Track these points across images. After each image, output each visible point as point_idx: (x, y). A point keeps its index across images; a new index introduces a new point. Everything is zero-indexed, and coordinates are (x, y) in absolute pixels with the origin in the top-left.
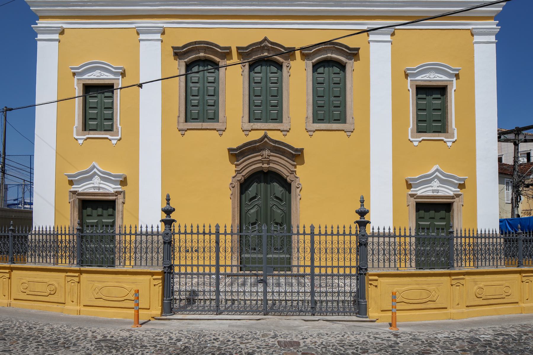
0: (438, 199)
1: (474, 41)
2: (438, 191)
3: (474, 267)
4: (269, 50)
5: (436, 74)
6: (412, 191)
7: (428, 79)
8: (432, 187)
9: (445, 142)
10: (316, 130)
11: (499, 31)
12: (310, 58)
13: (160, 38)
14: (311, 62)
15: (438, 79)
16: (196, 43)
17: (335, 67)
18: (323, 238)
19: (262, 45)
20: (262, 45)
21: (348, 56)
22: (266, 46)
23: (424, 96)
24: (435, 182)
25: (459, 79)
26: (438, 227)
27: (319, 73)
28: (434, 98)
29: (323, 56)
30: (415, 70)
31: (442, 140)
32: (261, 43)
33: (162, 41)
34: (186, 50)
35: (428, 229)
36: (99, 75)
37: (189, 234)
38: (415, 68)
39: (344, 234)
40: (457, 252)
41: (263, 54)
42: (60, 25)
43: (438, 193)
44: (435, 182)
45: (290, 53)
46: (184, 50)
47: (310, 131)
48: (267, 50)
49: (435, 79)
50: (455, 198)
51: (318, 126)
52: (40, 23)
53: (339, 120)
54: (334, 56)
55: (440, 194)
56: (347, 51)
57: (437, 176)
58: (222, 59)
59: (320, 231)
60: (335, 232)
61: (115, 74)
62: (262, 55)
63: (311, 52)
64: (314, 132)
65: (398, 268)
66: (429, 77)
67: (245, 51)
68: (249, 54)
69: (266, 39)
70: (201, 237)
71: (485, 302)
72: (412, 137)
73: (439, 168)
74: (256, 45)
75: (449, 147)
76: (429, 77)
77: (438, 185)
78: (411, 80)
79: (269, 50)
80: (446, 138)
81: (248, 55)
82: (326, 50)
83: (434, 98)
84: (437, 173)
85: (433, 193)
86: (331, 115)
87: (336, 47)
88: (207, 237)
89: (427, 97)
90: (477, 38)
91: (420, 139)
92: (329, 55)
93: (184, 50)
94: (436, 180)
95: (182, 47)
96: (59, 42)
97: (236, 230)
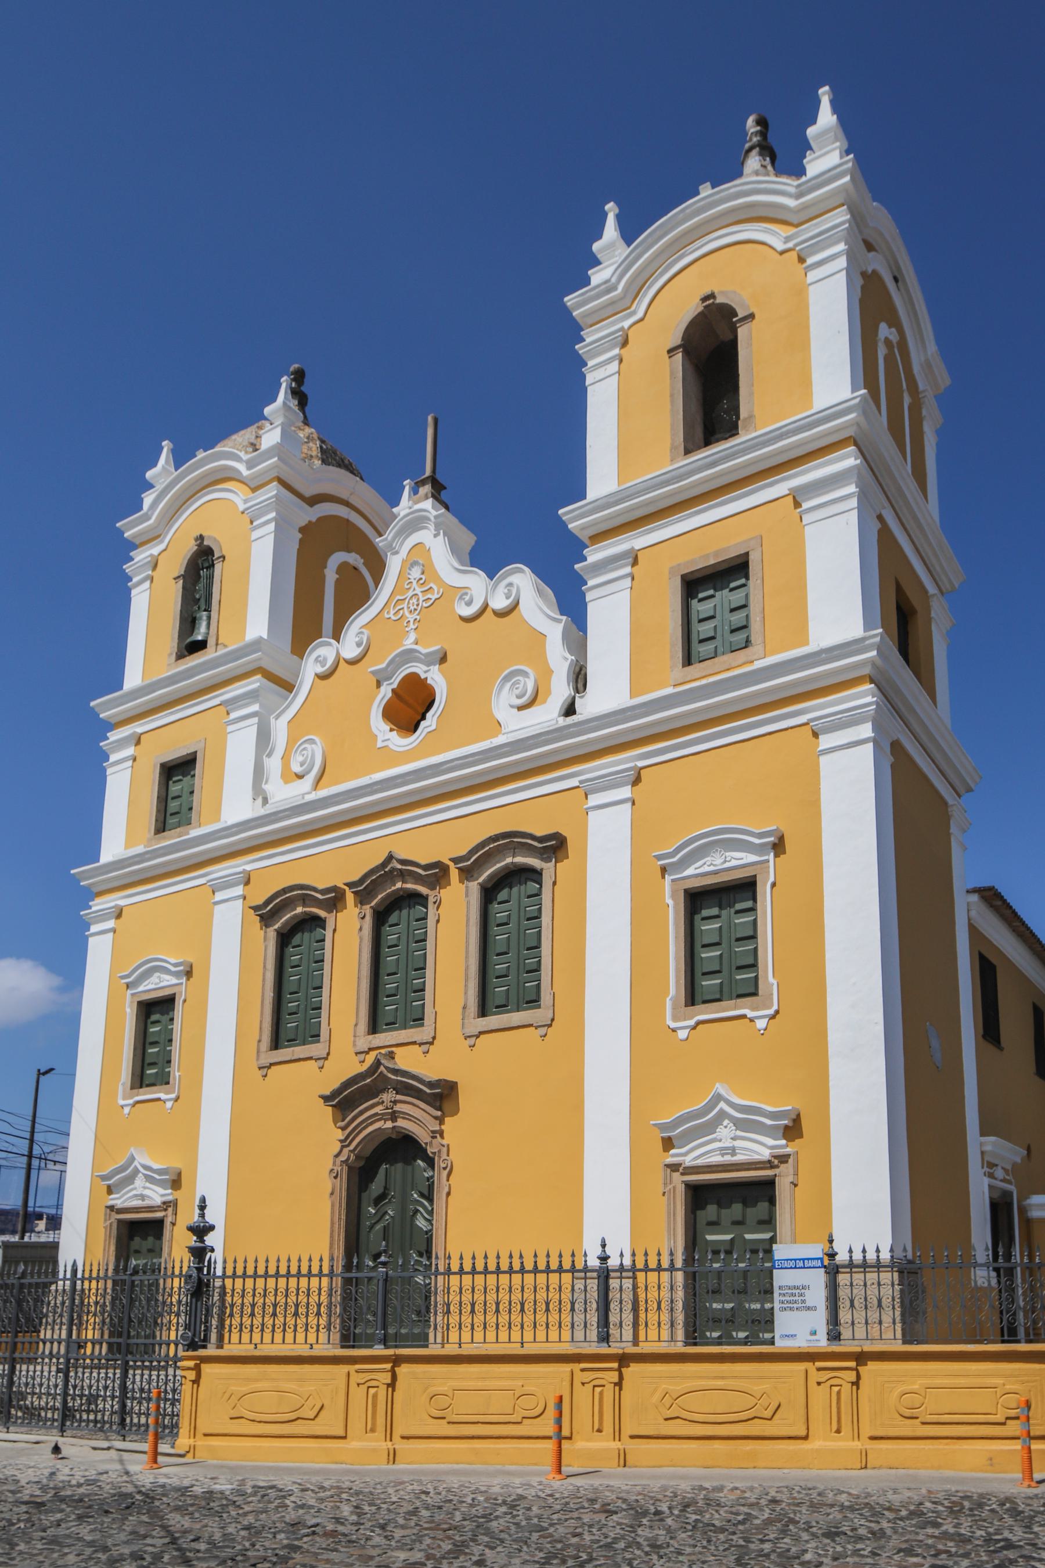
0: (738, 1170)
1: (820, 748)
2: (733, 1151)
3: (330, 1346)
4: (402, 875)
5: (727, 854)
6: (673, 1156)
7: (712, 868)
8: (720, 1140)
9: (752, 1020)
10: (481, 1033)
11: (876, 710)
12: (475, 876)
13: (241, 893)
14: (476, 882)
15: (734, 863)
16: (284, 891)
17: (529, 883)
18: (653, 1277)
19: (387, 870)
20: (387, 870)
21: (543, 854)
22: (393, 869)
23: (715, 911)
24: (726, 1127)
25: (784, 853)
26: (755, 1247)
27: (499, 903)
28: (737, 912)
29: (498, 866)
30: (673, 857)
31: (744, 1016)
32: (384, 864)
33: (245, 898)
34: (272, 908)
35: (729, 1252)
36: (157, 981)
37: (529, 1272)
38: (671, 850)
39: (474, 1272)
40: (232, 1310)
41: (395, 885)
42: (112, 904)
43: (734, 1154)
44: (726, 1127)
45: (437, 874)
46: (269, 908)
47: (469, 1037)
48: (397, 876)
49: (727, 865)
50: (777, 1167)
51: (484, 1023)
52: (96, 905)
53: (505, 1006)
54: (519, 860)
55: (739, 1158)
56: (535, 844)
57: (722, 1111)
58: (329, 913)
59: (536, 1262)
60: (480, 1267)
61: (176, 974)
62: (393, 888)
63: (469, 863)
64: (477, 1036)
65: (311, 1345)
66: (712, 864)
67: (359, 889)
68: (371, 891)
69: (390, 857)
70: (567, 1277)
71: (452, 1431)
72: (675, 1018)
73: (723, 1092)
74: (377, 872)
75: (762, 1032)
76: (712, 864)
77: (732, 1136)
78: (673, 881)
79: (402, 875)
80: (753, 1009)
81: (369, 894)
82: (500, 851)
83: (737, 912)
84: (722, 1105)
85: (723, 1155)
86: (521, 992)
87: (515, 840)
88: (665, 1276)
89: (724, 913)
90: (826, 741)
91: (692, 1022)
92: (509, 860)
93: (269, 908)
94: (726, 1122)
95: (264, 903)
96: (115, 932)
97: (339, 1269)
